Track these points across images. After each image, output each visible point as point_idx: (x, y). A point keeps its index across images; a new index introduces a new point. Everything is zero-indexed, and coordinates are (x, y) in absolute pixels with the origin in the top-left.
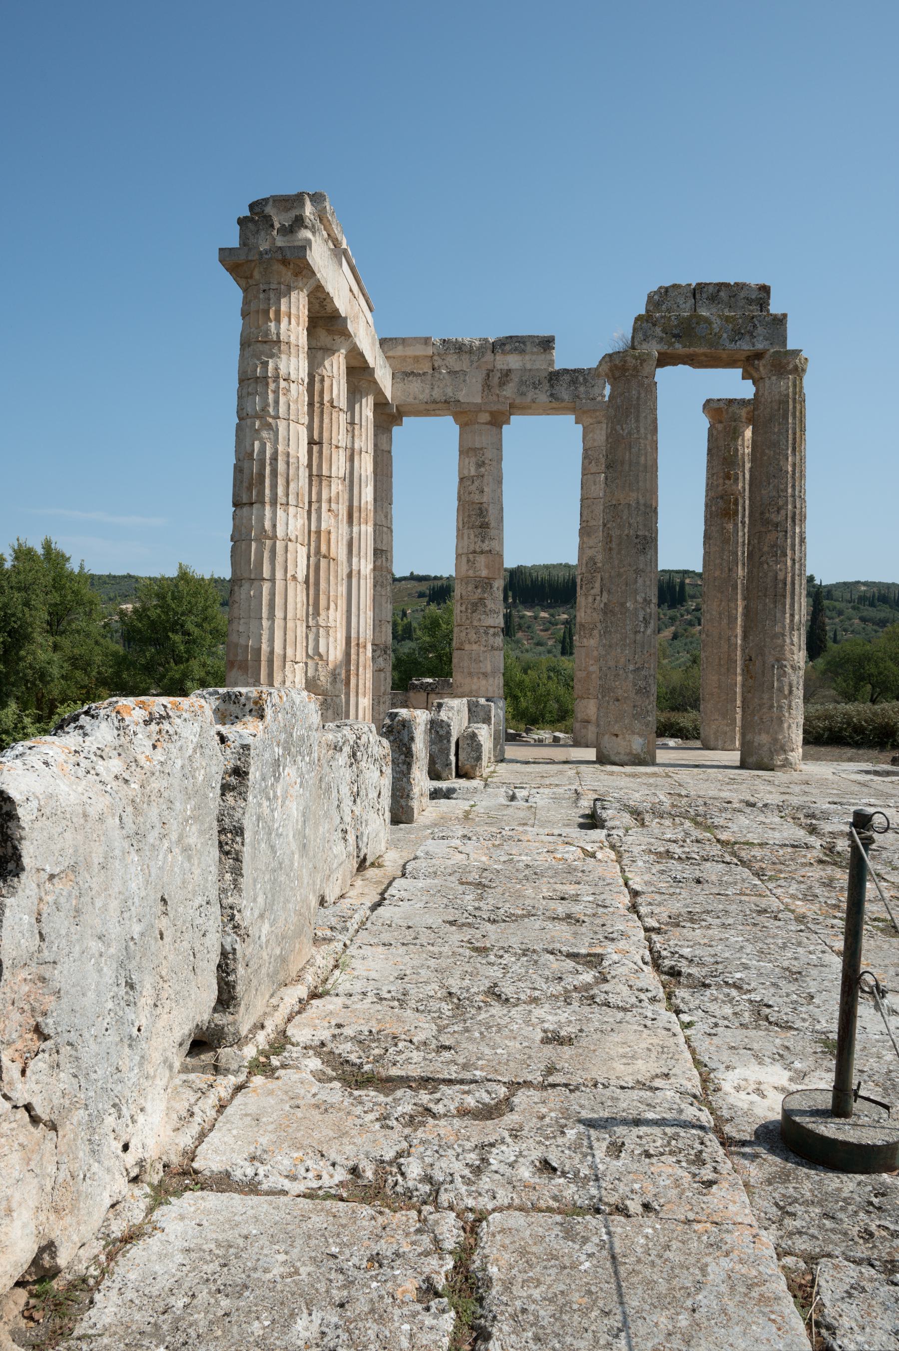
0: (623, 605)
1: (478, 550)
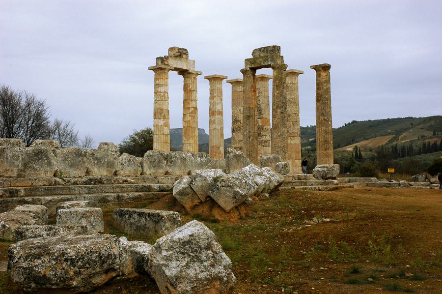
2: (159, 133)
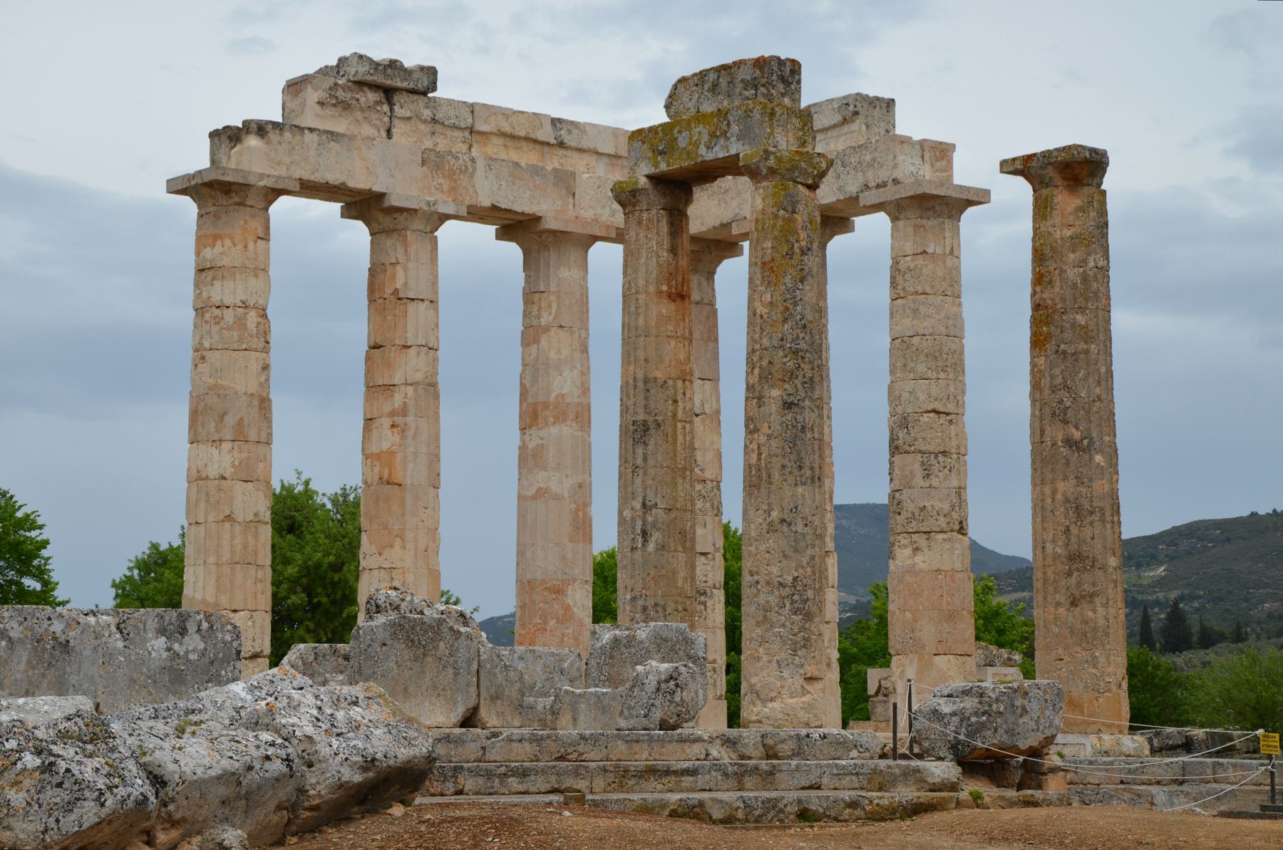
2: (211, 519)
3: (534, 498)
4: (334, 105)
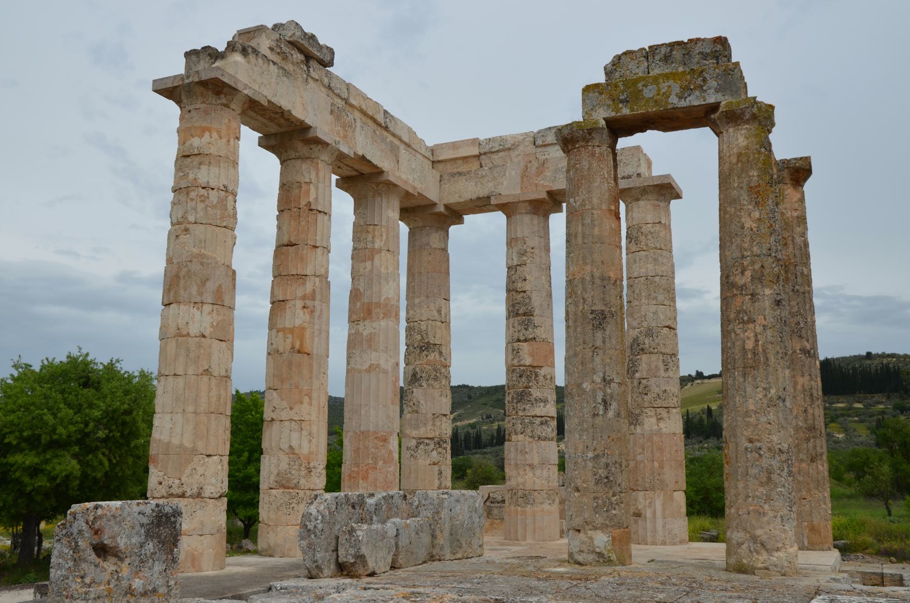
0: (579, 386)
1: (522, 338)
2: (190, 371)
3: (369, 370)
4: (278, 54)
